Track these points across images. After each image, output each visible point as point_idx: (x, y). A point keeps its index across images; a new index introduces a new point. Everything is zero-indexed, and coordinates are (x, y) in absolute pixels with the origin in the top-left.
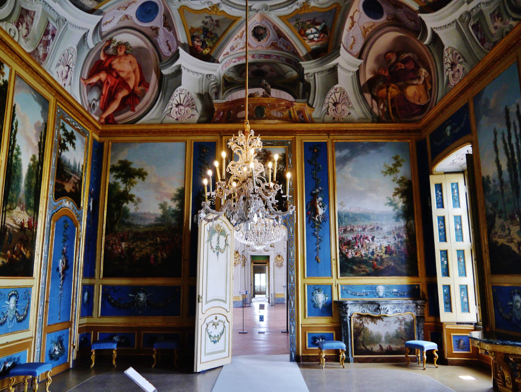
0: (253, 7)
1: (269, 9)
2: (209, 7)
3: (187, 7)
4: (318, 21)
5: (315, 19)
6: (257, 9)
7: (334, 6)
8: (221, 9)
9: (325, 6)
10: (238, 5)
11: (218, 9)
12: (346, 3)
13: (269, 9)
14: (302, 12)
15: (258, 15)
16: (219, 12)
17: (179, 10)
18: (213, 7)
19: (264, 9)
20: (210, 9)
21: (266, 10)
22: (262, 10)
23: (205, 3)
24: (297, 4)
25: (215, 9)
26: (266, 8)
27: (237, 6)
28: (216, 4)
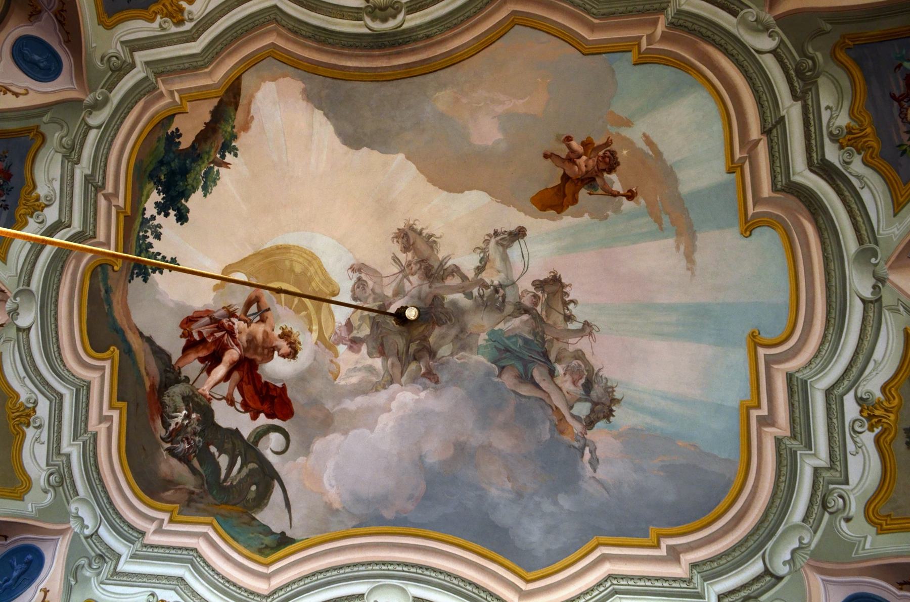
0: (867, 294)
1: (873, 245)
2: (871, 429)
3: (869, 503)
4: (902, 83)
5: (893, 97)
6: (873, 281)
7: (842, 56)
8: (878, 394)
9: (846, 83)
10: (861, 339)
11: (880, 402)
12: (829, 27)
13: (873, 245)
14: (875, 144)
15: (895, 278)
16: (888, 400)
17: (881, 531)
18: (870, 417)
19: (873, 260)
20: (877, 431)
21: (875, 254)
22: (876, 265)
23: (855, 442)
24: (848, 163)
25: (877, 413)
26: (866, 254)
27: (866, 345)
28: (859, 408)
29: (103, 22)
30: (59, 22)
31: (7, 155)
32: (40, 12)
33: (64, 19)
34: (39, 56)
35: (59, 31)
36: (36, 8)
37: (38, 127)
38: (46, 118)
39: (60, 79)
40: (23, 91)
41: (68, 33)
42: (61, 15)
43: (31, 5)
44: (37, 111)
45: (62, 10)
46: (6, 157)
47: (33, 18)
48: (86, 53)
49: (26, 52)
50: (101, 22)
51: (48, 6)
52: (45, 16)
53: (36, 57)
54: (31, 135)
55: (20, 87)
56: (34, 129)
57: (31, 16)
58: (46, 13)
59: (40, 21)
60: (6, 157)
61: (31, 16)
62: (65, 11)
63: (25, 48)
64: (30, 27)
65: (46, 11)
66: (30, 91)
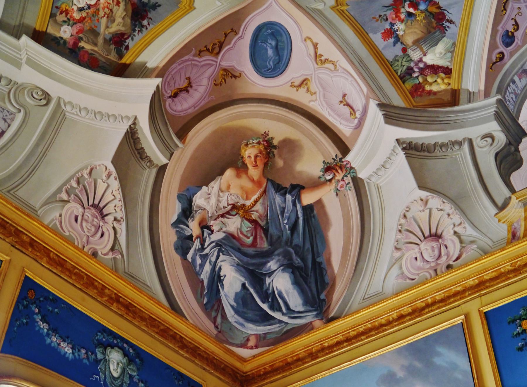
29: (189, 6)
30: (221, 47)
31: (378, 16)
32: (225, 70)
33: (214, 44)
34: (267, 50)
35: (229, 44)
36: (224, 75)
37: (332, 8)
38: (320, 6)
39: (274, 19)
40: (309, 42)
41: (226, 35)
42: (213, 49)
43: (225, 81)
44: (319, 20)
45: (208, 50)
46: (380, 16)
47: (237, 74)
48: (233, 7)
49: (271, 63)
50: (191, 8)
51: (213, 65)
52: (225, 64)
53: (270, 52)
54: (344, 8)
55: (306, 47)
56: (337, 10)
57: (235, 77)
58: (221, 63)
59: (233, 66)
60: (380, 16)
61: (235, 77)
62: (206, 47)
63: (269, 67)
64: (246, 72)
65: (219, 64)
66: (304, 37)
